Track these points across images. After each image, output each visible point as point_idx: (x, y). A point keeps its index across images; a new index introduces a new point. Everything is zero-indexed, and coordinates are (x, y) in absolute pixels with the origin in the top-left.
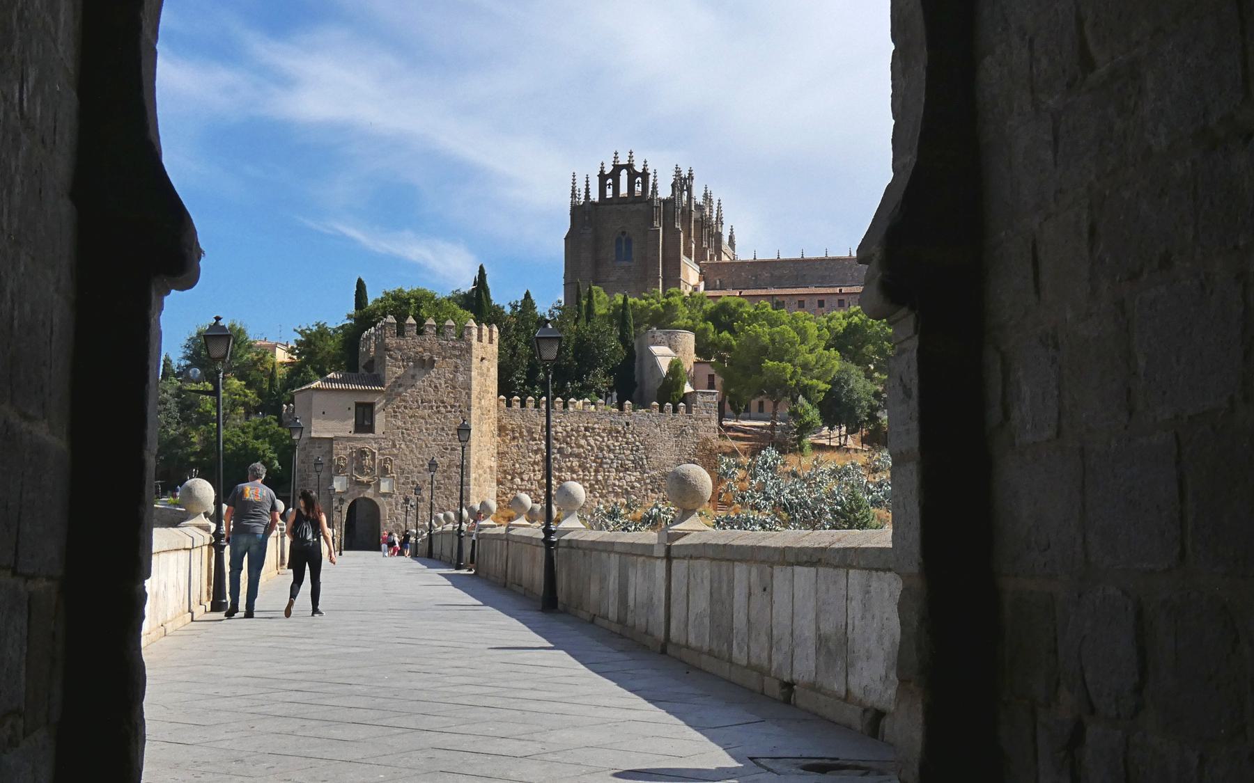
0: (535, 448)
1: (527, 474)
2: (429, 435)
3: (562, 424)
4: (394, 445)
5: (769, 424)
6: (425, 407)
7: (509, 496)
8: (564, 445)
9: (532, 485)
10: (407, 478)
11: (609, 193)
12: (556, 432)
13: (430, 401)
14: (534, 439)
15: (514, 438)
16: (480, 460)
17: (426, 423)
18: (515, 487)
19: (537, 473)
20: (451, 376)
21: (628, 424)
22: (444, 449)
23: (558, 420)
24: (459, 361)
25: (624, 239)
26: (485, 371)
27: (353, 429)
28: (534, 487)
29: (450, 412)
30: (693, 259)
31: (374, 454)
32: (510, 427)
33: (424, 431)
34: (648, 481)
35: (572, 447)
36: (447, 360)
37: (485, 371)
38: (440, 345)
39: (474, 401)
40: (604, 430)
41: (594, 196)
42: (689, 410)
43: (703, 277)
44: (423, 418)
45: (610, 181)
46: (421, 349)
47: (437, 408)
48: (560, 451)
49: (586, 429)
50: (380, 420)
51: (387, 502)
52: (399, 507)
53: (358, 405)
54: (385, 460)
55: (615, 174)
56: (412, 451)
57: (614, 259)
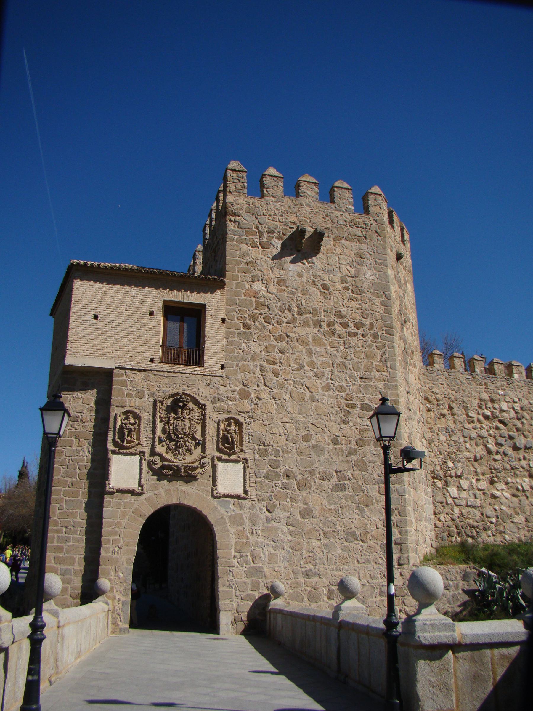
1: (467, 479)
2: (316, 375)
3: (508, 399)
6: (306, 323)
8: (515, 434)
9: (476, 497)
10: (275, 464)
12: (502, 411)
13: (315, 312)
18: (450, 500)
19: (481, 477)
20: (352, 270)
22: (347, 406)
23: (501, 392)
24: (364, 247)
28: (478, 503)
29: (356, 335)
31: (202, 407)
33: (307, 368)
36: (343, 241)
38: (327, 216)
44: (305, 342)
47: (329, 325)
51: (230, 517)
52: (259, 527)
56: (281, 407)
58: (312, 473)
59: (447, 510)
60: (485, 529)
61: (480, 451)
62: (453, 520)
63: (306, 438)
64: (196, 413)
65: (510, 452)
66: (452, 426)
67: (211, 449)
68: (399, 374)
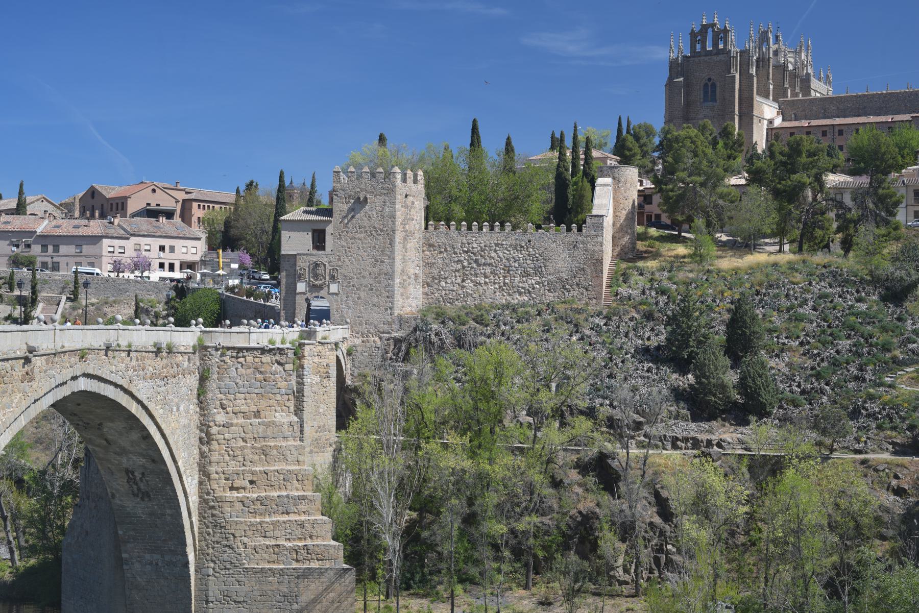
0: (456, 259)
4: (339, 260)
5: (683, 234)
6: (361, 232)
7: (436, 295)
10: (349, 283)
11: (698, 47)
12: (473, 248)
13: (365, 227)
14: (455, 253)
15: (441, 252)
16: (405, 269)
17: (363, 243)
18: (441, 288)
21: (529, 241)
24: (387, 198)
25: (709, 84)
26: (410, 204)
28: (455, 288)
30: (771, 98)
31: (325, 265)
32: (436, 244)
34: (546, 284)
35: (485, 259)
37: (410, 204)
39: (399, 227)
40: (511, 245)
42: (580, 230)
43: (782, 112)
46: (358, 190)
48: (476, 261)
49: (497, 245)
52: (343, 303)
54: (333, 269)
56: (352, 263)
57: (702, 100)
58: (361, 285)
59: (440, 292)
60: (457, 300)
61: (459, 266)
62: (441, 296)
63: (360, 274)
64: (323, 267)
65: (475, 265)
66: (445, 256)
67: (327, 278)
68: (398, 247)
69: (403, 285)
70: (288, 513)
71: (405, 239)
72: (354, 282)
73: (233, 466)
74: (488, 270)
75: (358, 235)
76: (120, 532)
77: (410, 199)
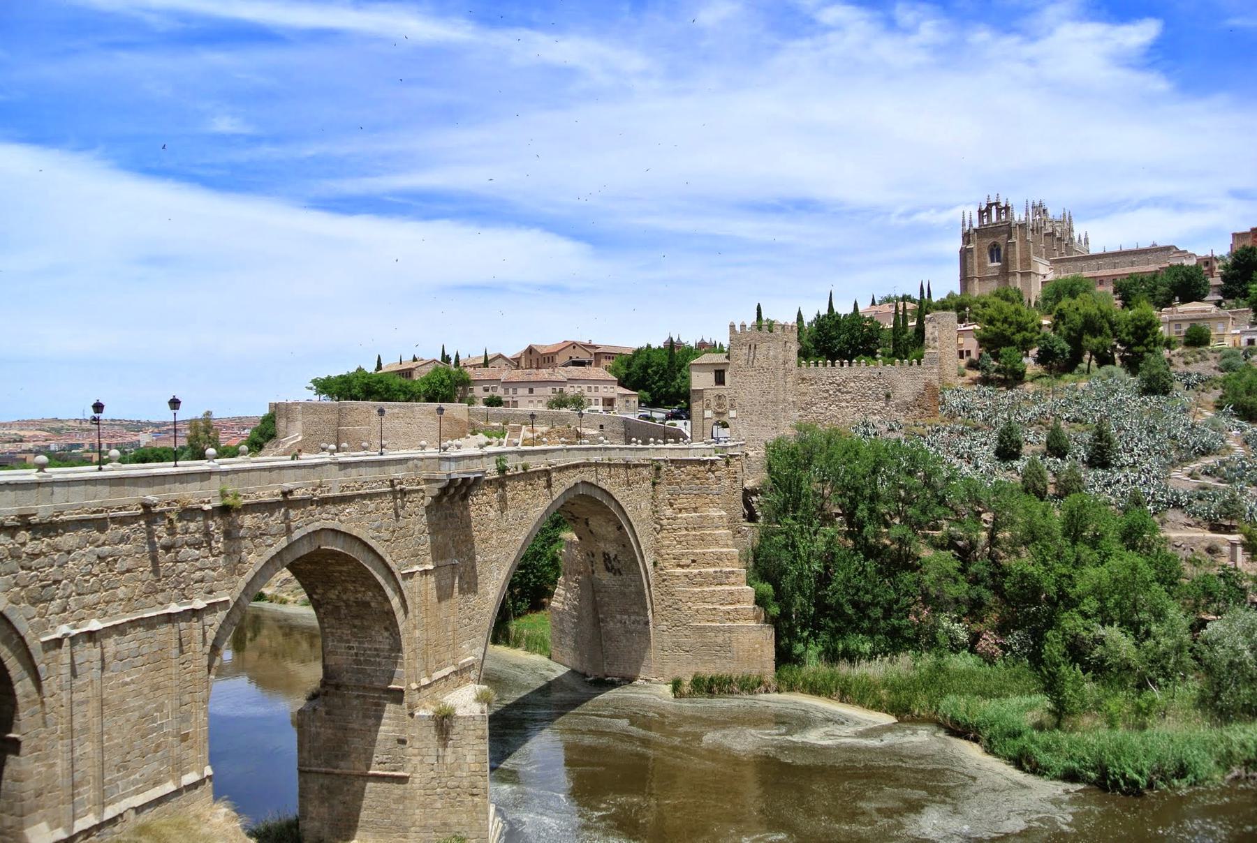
15: (812, 385)
27: (714, 383)
41: (976, 225)
42: (919, 363)
45: (985, 214)
50: (727, 377)
53: (716, 371)
55: (988, 210)
69: (784, 410)
70: (721, 584)
71: (785, 375)
72: (748, 408)
73: (678, 550)
74: (848, 397)
75: (750, 373)
76: (598, 599)
77: (788, 344)
